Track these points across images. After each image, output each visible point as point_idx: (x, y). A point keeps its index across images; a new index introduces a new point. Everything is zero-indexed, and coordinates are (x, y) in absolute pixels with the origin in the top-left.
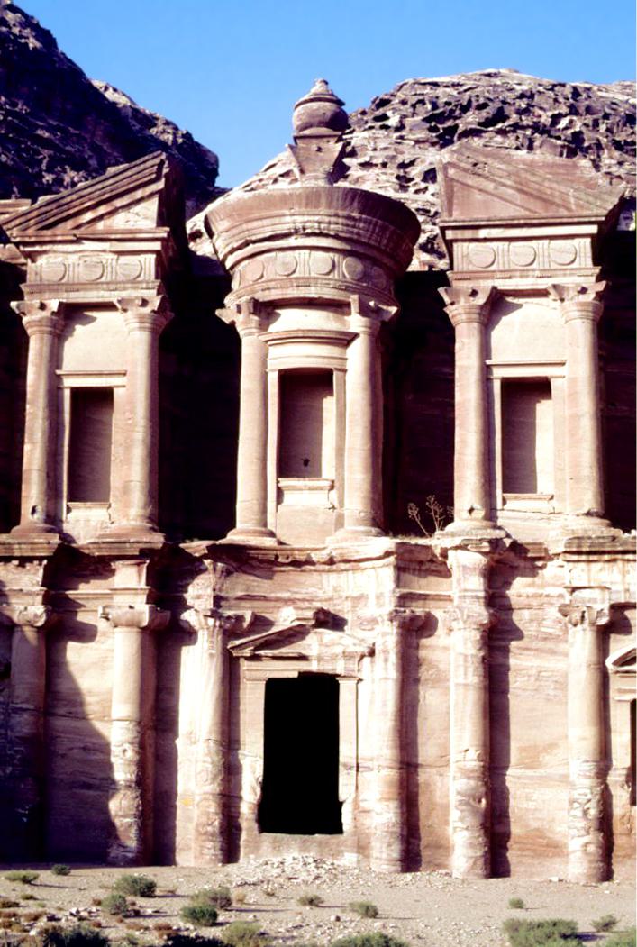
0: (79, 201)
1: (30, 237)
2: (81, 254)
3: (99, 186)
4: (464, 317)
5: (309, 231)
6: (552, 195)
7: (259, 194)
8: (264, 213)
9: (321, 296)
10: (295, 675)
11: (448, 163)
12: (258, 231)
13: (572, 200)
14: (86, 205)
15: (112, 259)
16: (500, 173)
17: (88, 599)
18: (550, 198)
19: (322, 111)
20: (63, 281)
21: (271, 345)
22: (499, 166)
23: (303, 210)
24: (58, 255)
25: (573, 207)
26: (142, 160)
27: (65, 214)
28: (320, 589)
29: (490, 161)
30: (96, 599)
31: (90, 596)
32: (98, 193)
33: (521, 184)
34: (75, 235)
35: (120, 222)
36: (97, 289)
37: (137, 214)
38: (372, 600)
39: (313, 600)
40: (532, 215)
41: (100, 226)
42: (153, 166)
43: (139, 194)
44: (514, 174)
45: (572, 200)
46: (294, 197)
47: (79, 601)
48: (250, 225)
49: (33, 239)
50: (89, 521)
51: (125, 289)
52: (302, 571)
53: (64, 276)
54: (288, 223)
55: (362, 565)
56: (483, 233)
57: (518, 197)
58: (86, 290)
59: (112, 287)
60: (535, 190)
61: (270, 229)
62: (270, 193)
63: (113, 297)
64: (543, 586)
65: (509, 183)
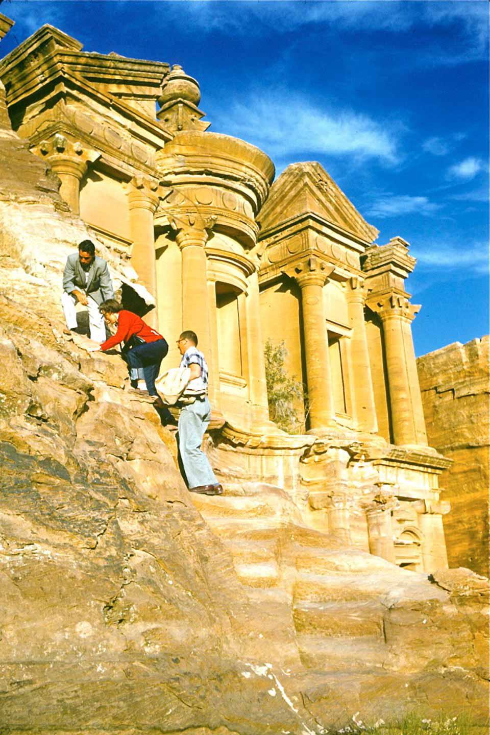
0: (112, 71)
1: (77, 80)
3: (129, 66)
5: (251, 183)
11: (308, 173)
14: (117, 77)
16: (331, 192)
21: (209, 259)
24: (87, 109)
26: (158, 63)
27: (101, 76)
34: (111, 101)
42: (162, 73)
43: (147, 90)
45: (359, 227)
49: (78, 84)
51: (138, 168)
52: (236, 452)
59: (131, 162)
61: (230, 170)
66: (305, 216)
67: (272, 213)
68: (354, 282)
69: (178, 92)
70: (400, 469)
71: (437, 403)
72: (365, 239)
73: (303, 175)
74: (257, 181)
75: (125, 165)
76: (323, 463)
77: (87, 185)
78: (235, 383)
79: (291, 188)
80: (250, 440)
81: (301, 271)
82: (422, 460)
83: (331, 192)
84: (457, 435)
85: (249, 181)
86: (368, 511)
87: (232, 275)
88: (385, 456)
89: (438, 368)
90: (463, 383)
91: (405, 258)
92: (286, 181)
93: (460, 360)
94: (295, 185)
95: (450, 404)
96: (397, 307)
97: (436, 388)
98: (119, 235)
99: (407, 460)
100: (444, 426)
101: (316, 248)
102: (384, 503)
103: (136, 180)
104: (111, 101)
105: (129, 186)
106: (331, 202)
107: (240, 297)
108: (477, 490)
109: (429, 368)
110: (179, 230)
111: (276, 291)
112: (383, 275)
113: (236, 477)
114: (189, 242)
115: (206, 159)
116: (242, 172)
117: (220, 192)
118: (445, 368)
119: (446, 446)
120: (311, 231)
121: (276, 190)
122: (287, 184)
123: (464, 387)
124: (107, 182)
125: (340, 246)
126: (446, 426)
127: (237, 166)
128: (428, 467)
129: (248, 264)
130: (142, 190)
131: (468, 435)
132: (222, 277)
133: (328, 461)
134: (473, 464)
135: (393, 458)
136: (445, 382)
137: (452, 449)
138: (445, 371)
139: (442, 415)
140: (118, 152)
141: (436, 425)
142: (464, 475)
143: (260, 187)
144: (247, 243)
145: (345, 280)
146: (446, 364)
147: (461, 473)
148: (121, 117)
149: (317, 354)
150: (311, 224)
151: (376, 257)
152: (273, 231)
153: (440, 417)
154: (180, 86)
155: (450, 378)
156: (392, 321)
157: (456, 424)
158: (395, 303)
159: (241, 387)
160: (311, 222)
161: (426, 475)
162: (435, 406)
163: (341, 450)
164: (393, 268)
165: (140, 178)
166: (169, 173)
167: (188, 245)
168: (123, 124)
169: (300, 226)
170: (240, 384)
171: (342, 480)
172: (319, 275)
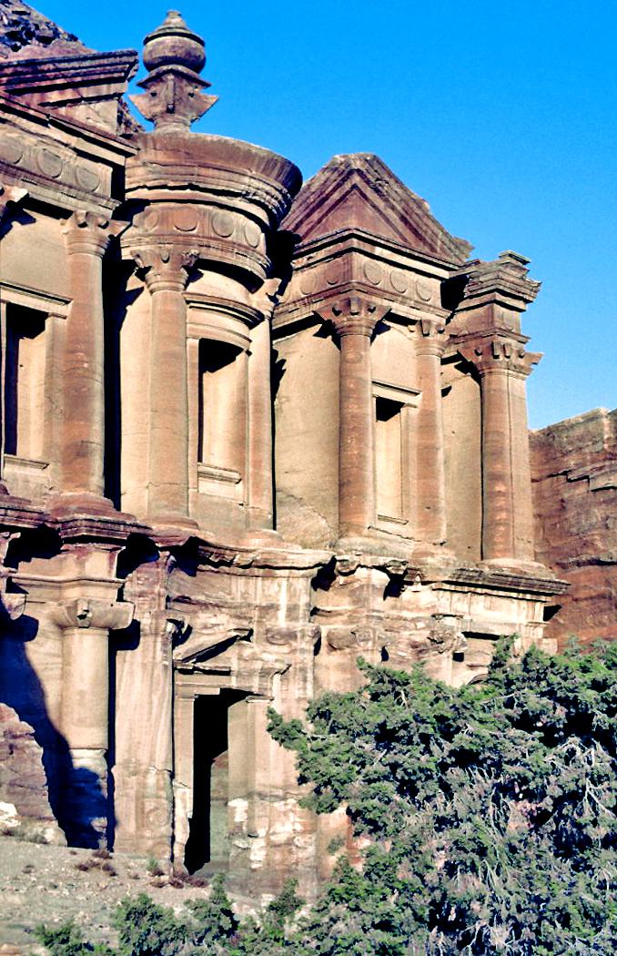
2: (40, 139)
4: (364, 330)
5: (257, 198)
6: (426, 232)
7: (226, 141)
8: (226, 166)
9: (253, 271)
10: (217, 692)
11: (358, 170)
12: (216, 181)
13: (439, 243)
14: (59, 82)
15: (71, 157)
16: (394, 195)
17: (31, 586)
18: (423, 234)
19: (198, 54)
20: (18, 165)
21: (191, 307)
22: (398, 190)
23: (259, 175)
25: (438, 250)
28: (229, 594)
29: (392, 182)
30: (41, 586)
31: (34, 582)
32: (72, 71)
33: (406, 212)
34: (48, 116)
35: (80, 113)
36: (56, 190)
37: (97, 113)
38: (282, 613)
39: (222, 607)
40: (407, 245)
41: (63, 111)
42: (125, 63)
44: (405, 201)
45: (439, 243)
46: (257, 158)
47: (22, 587)
48: (203, 171)
50: (28, 482)
53: (18, 161)
54: (245, 184)
55: (278, 572)
56: (378, 251)
57: (400, 225)
58: (44, 186)
59: (73, 192)
60: (415, 223)
61: (226, 183)
62: (237, 145)
63: (66, 202)
64: (402, 608)
65: (399, 208)
66: (347, 233)
67: (306, 222)
68: (425, 326)
69: (171, 54)
70: (476, 596)
71: (566, 496)
72: (449, 260)
73: (351, 172)
74: (267, 193)
75: (64, 198)
76: (350, 587)
77: (13, 229)
78: (223, 479)
79: (334, 190)
80: (237, 557)
81: (340, 312)
82: (512, 583)
83: (394, 195)
84: (585, 544)
85: (254, 194)
86: (420, 651)
87: (226, 328)
88: (446, 579)
89: (571, 443)
90: (601, 468)
91: (521, 282)
92: (328, 179)
93: (601, 435)
94: (339, 185)
95: (583, 498)
96: (501, 358)
97: (565, 473)
98: (53, 292)
99: (486, 583)
100: (571, 530)
101: (364, 280)
102: (441, 642)
103: (76, 216)
104: (48, 116)
105: (69, 225)
106: (393, 208)
107: (240, 358)
108: (604, 625)
109: (560, 443)
110: (148, 269)
111: (315, 335)
112: (486, 307)
113: (217, 606)
114: (161, 284)
115: (190, 170)
116: (245, 183)
117: (210, 213)
118: (581, 444)
119: (571, 560)
120: (356, 255)
121: (313, 190)
122: (328, 183)
123: (603, 474)
124: (43, 221)
125: (406, 272)
126: (574, 530)
127: (236, 177)
128: (525, 592)
129: (248, 311)
130: (86, 229)
131: (599, 544)
132: (207, 332)
133: (356, 585)
134: (603, 588)
135: (461, 580)
136: (580, 465)
137: (579, 564)
138: (581, 449)
139: (571, 514)
140: (52, 181)
141: (562, 527)
142: (590, 601)
143: (273, 201)
144: (251, 283)
145: (413, 322)
146: (581, 439)
147: (586, 599)
148: (63, 133)
149: (354, 434)
150: (355, 246)
151: (475, 280)
152: (306, 249)
153: (567, 516)
154: (173, 47)
155: (584, 459)
156: (494, 377)
157: (586, 528)
158: (498, 352)
159: (233, 484)
160: (355, 243)
161: (524, 604)
162: (563, 501)
163: (374, 570)
164: (499, 297)
165: (82, 214)
166: (139, 187)
167: (160, 289)
168: (65, 142)
169: (341, 246)
170: (229, 480)
171: (374, 611)
172: (365, 320)
